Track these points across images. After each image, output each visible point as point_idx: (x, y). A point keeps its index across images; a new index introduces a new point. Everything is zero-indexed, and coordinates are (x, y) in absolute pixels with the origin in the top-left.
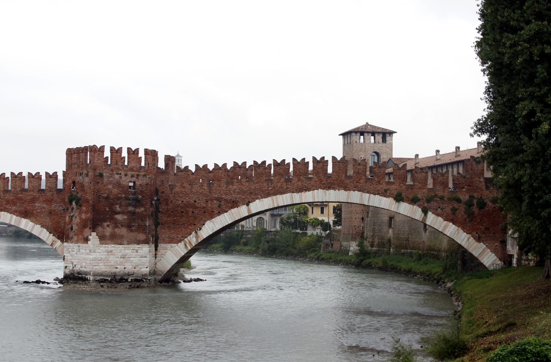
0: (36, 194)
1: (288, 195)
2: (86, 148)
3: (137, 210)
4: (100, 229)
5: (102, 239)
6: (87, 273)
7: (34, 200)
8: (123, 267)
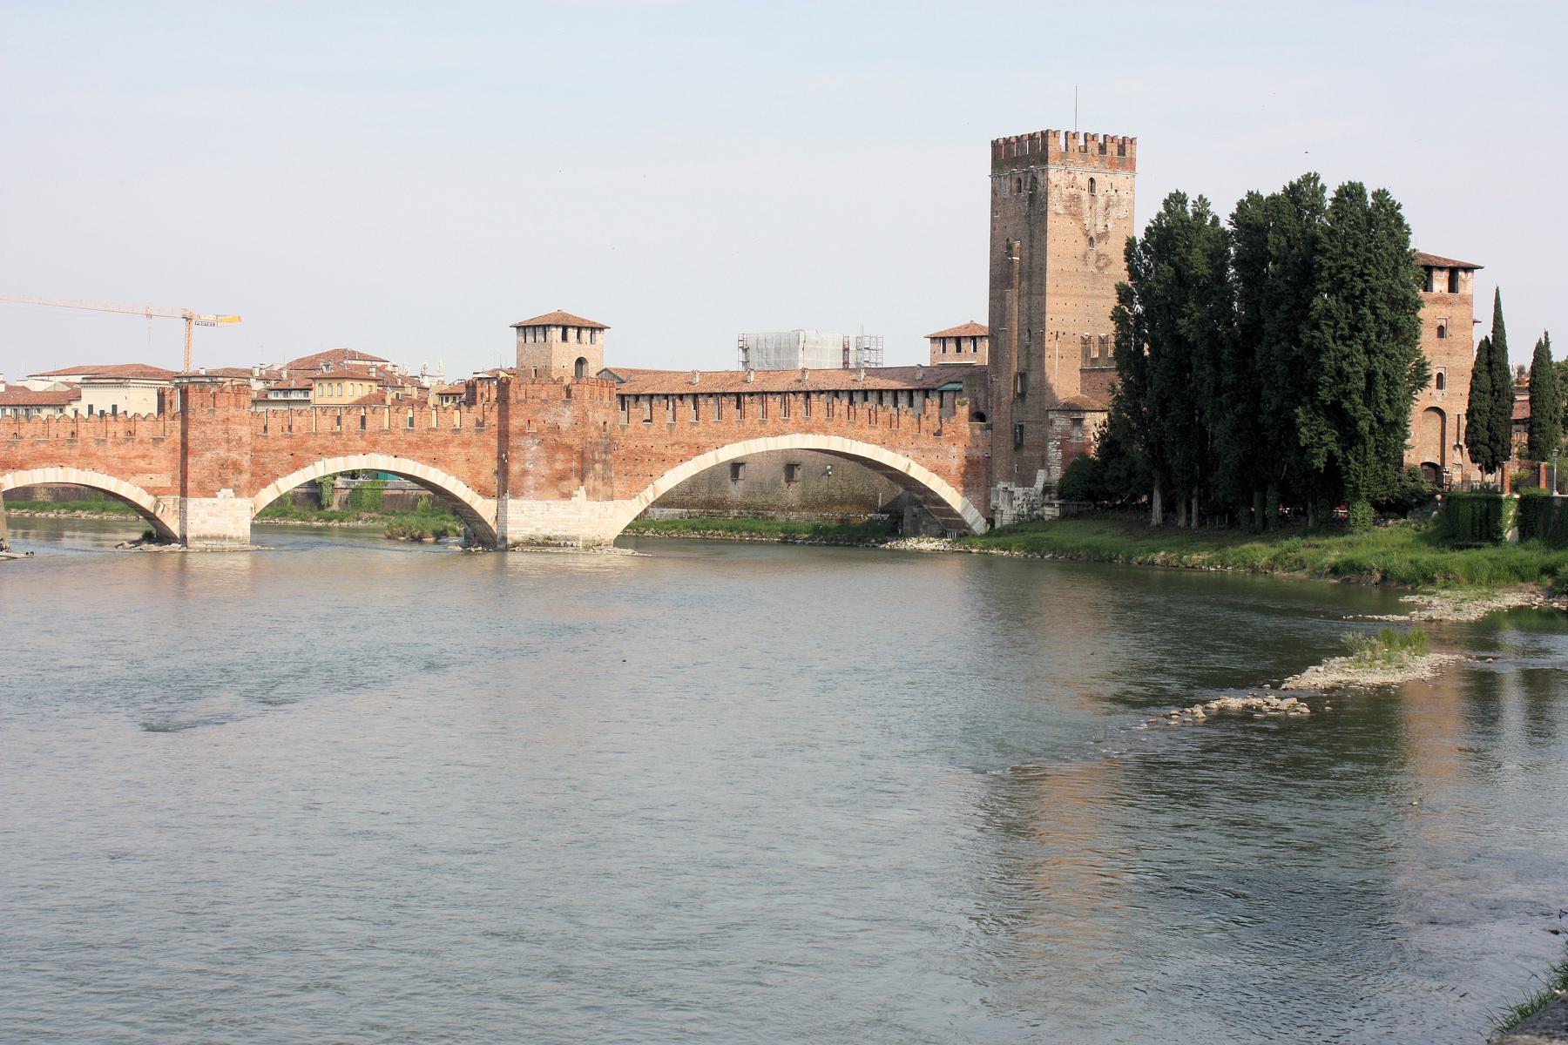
0: (449, 435)
1: (762, 440)
5: (592, 494)
6: (576, 538)
7: (446, 443)
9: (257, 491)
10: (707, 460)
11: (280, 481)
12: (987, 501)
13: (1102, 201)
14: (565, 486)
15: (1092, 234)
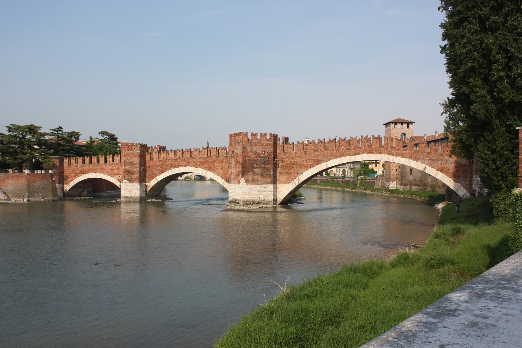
2: (238, 134)
3: (266, 166)
4: (246, 176)
5: (247, 181)
6: (240, 200)
7: (214, 162)
8: (258, 197)
9: (150, 180)
10: (322, 166)
11: (157, 177)
12: (471, 185)
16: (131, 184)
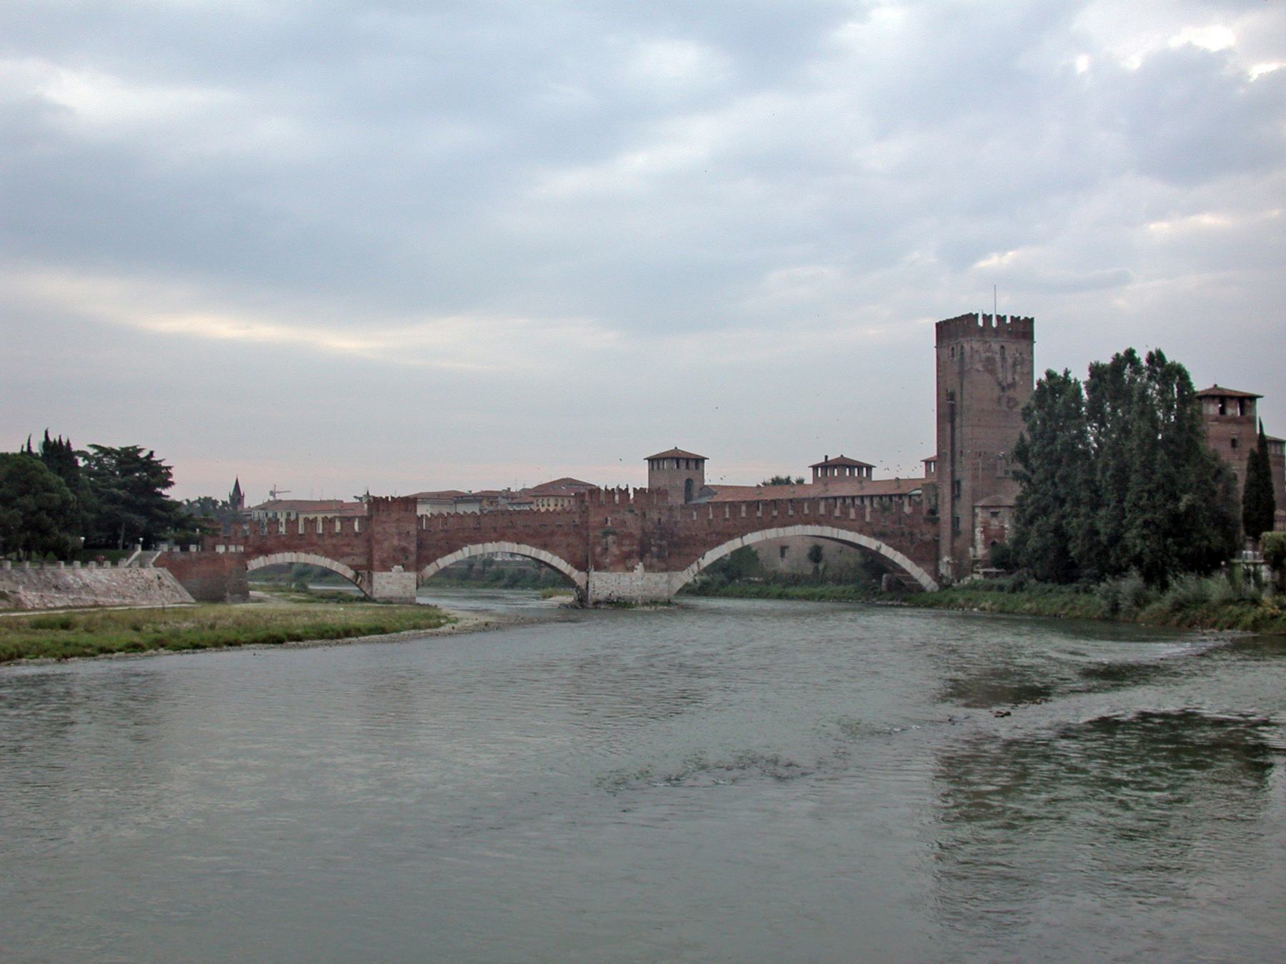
5: (648, 568)
7: (552, 534)
11: (439, 561)
12: (937, 569)
13: (1010, 361)
14: (629, 564)
15: (1004, 384)
16: (407, 574)
